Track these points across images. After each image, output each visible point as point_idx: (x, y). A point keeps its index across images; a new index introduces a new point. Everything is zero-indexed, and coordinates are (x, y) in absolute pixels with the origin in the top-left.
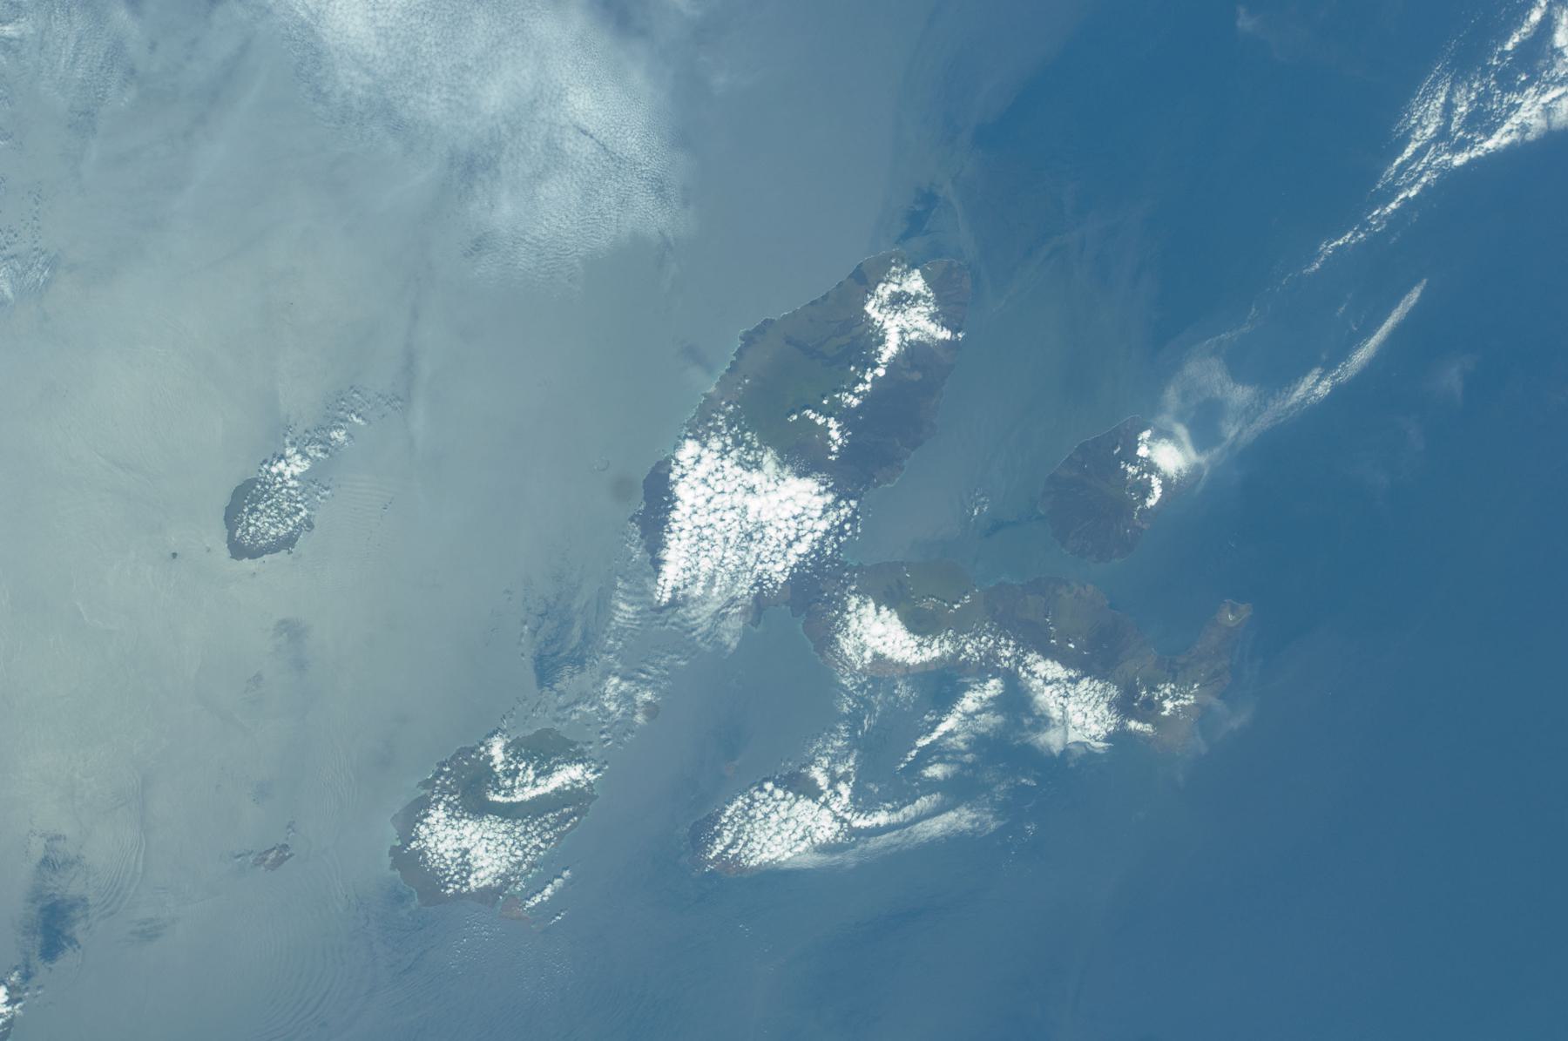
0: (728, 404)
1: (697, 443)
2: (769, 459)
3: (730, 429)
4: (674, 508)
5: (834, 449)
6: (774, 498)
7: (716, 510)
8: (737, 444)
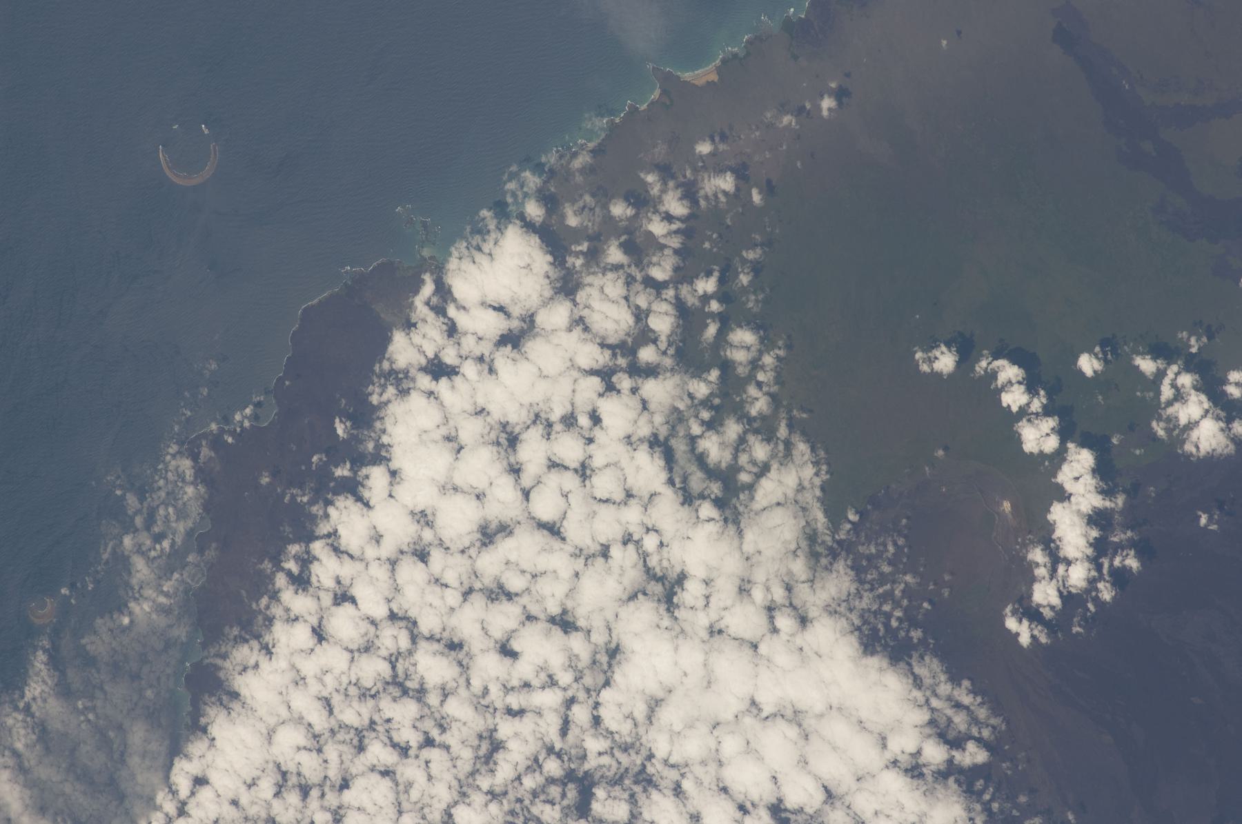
0: (716, 165)
1: (541, 261)
2: (786, 486)
3: (683, 276)
4: (353, 488)
5: (1045, 594)
6: (735, 676)
7: (499, 593)
8: (690, 354)
